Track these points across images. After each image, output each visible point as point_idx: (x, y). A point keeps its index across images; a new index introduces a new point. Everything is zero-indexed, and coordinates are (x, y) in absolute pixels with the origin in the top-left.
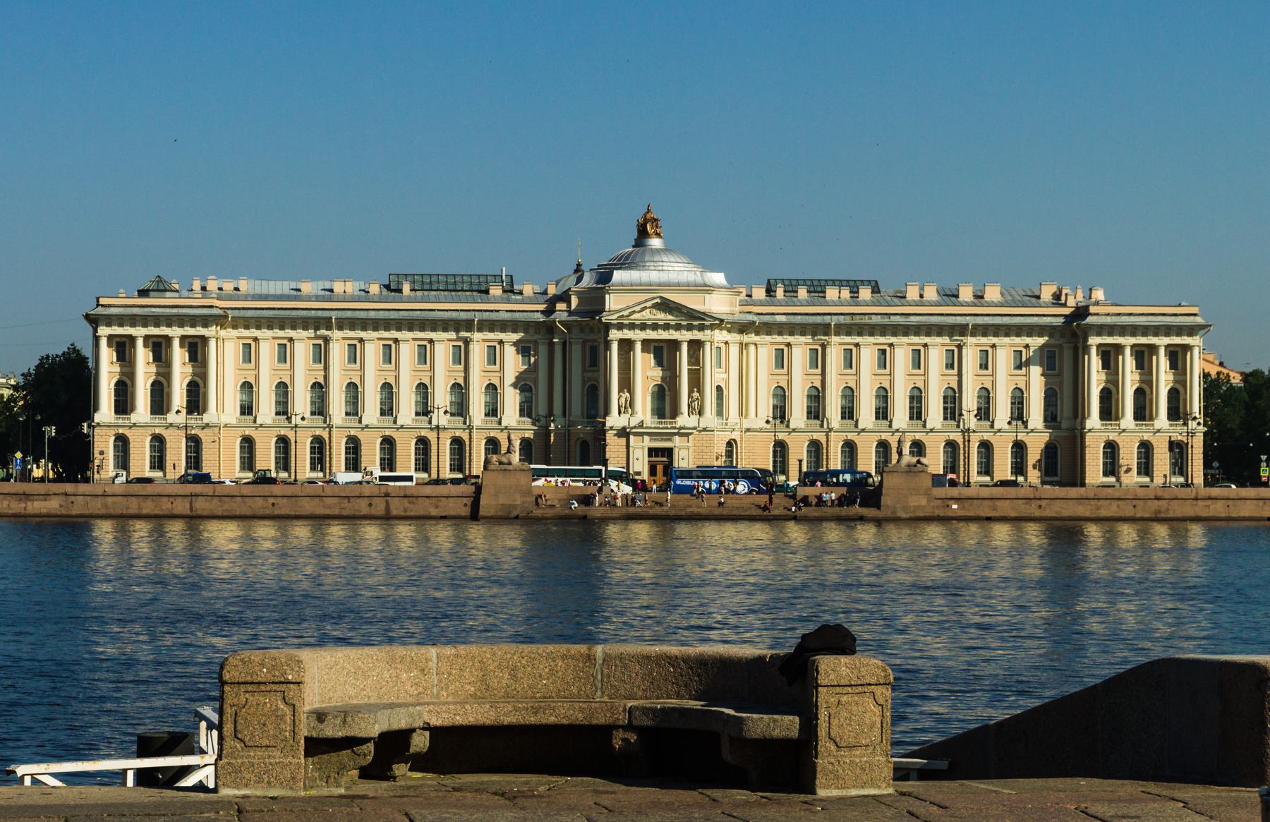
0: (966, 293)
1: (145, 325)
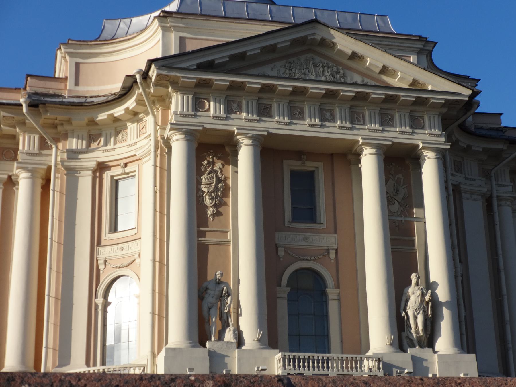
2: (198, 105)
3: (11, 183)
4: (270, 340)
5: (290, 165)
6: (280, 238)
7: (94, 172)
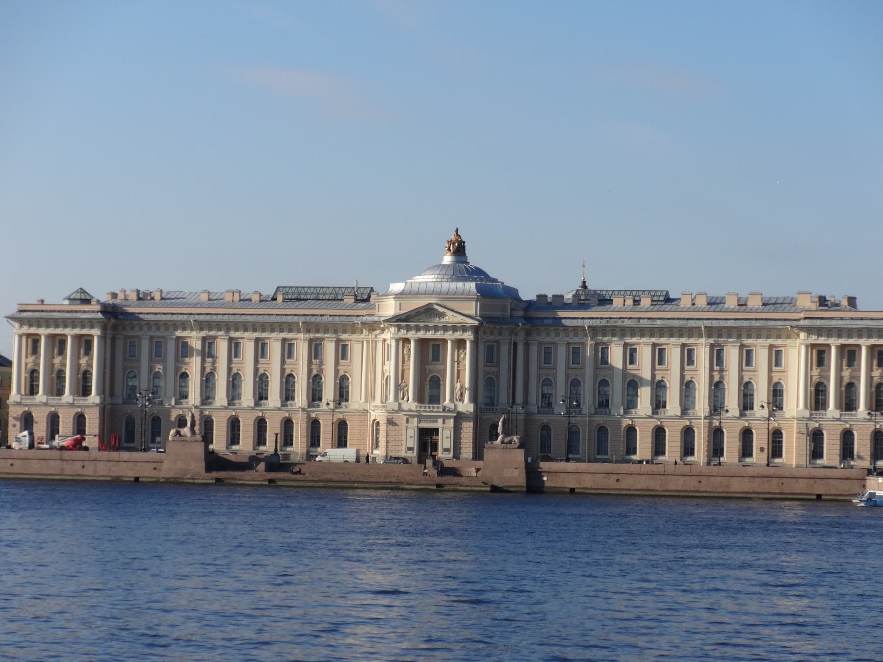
0: (731, 303)
1: (48, 326)
4: (414, 400)
6: (428, 367)
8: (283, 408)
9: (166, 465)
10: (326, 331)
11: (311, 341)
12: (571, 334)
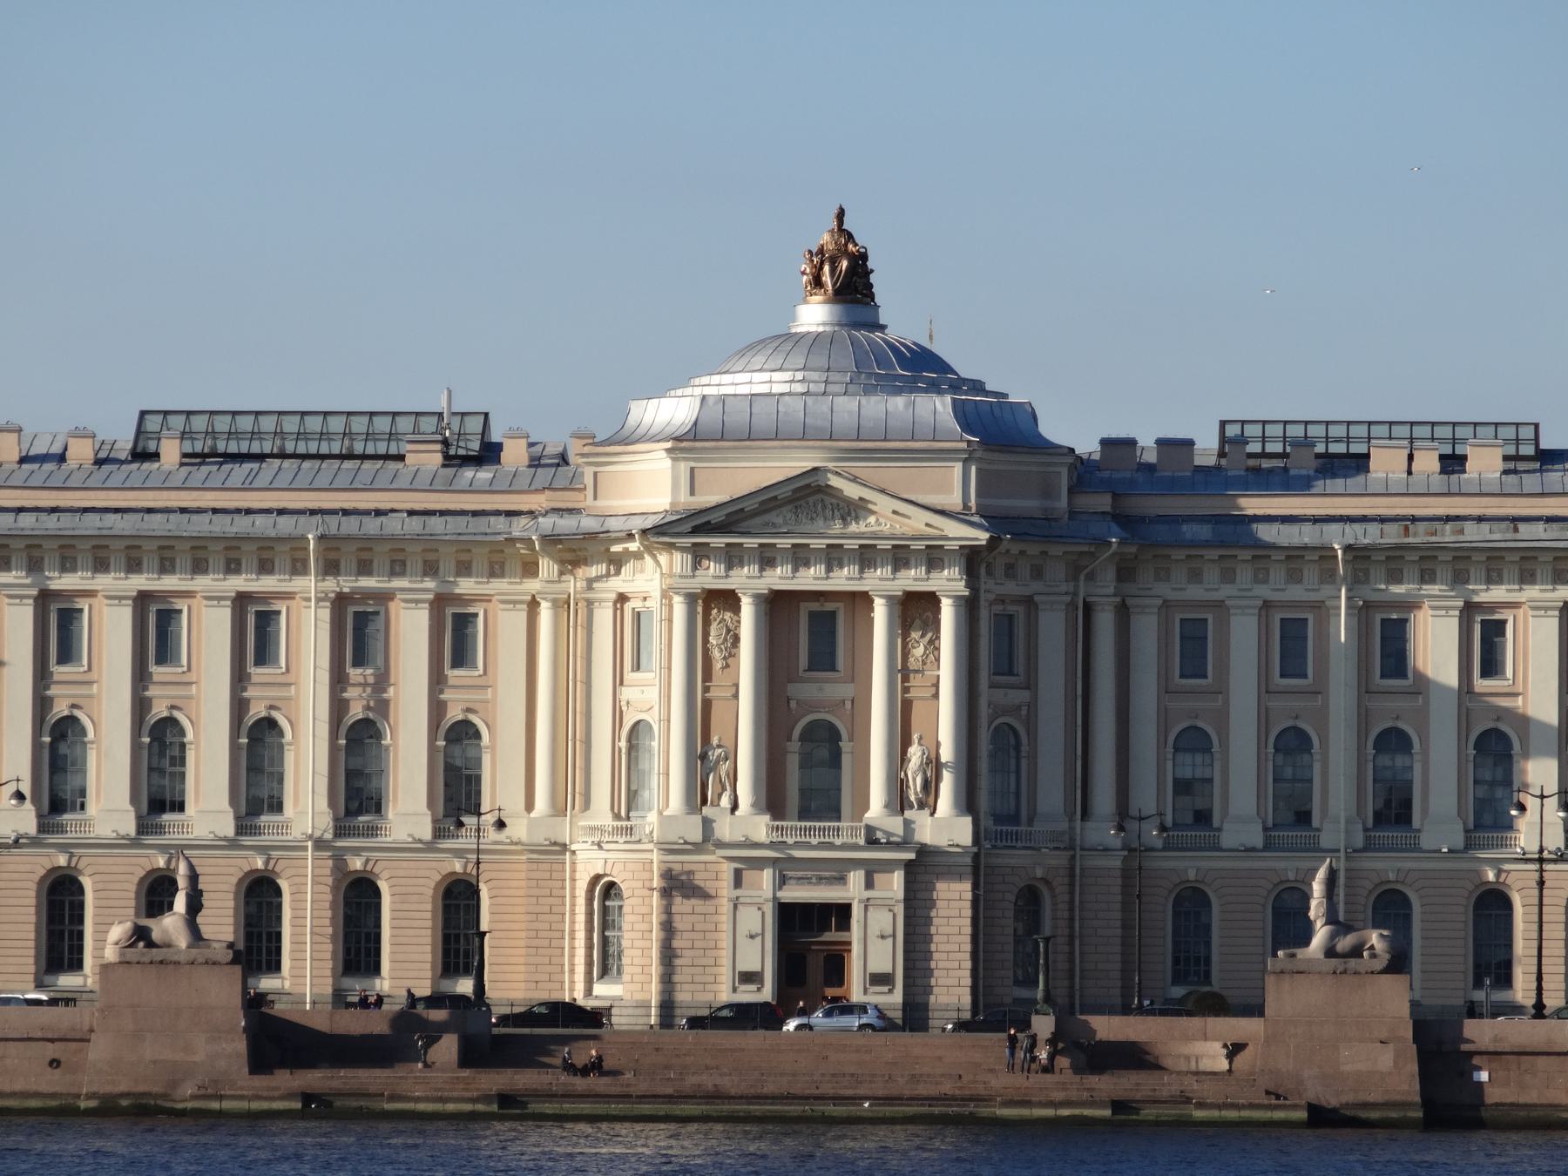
2: (696, 564)
3: (533, 605)
5: (806, 607)
6: (792, 689)
7: (615, 603)
8: (247, 841)
9: (98, 1051)
10: (397, 568)
11: (340, 603)
12: (1277, 574)
